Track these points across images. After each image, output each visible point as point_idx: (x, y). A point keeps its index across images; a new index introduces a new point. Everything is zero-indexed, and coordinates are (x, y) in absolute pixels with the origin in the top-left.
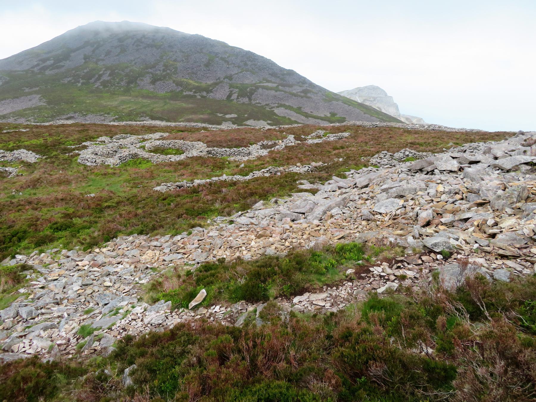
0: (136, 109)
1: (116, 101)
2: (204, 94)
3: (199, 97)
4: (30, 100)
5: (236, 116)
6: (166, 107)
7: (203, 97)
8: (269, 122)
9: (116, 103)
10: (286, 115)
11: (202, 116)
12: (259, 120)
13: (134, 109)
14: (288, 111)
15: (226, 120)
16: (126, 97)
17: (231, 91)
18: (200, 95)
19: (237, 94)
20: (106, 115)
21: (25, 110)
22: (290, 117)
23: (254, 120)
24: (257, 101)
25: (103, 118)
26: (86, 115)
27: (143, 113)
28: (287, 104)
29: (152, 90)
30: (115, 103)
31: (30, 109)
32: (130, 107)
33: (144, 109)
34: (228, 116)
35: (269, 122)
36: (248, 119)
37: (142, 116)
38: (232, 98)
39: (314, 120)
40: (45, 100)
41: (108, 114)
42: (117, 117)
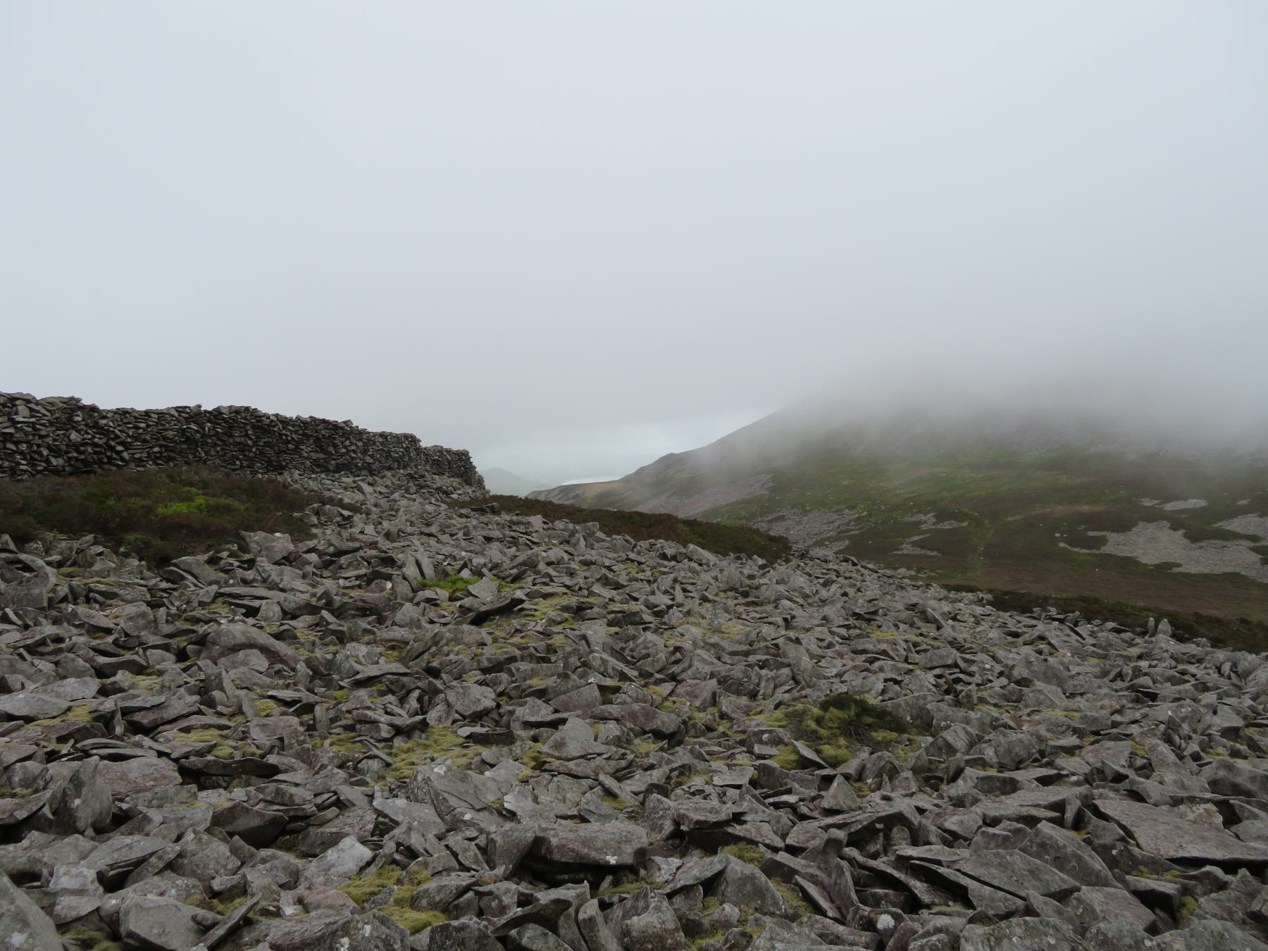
11: (1086, 508)
15: (1152, 517)
23: (1261, 516)
26: (805, 513)
34: (1169, 507)
36: (1243, 511)
41: (852, 508)
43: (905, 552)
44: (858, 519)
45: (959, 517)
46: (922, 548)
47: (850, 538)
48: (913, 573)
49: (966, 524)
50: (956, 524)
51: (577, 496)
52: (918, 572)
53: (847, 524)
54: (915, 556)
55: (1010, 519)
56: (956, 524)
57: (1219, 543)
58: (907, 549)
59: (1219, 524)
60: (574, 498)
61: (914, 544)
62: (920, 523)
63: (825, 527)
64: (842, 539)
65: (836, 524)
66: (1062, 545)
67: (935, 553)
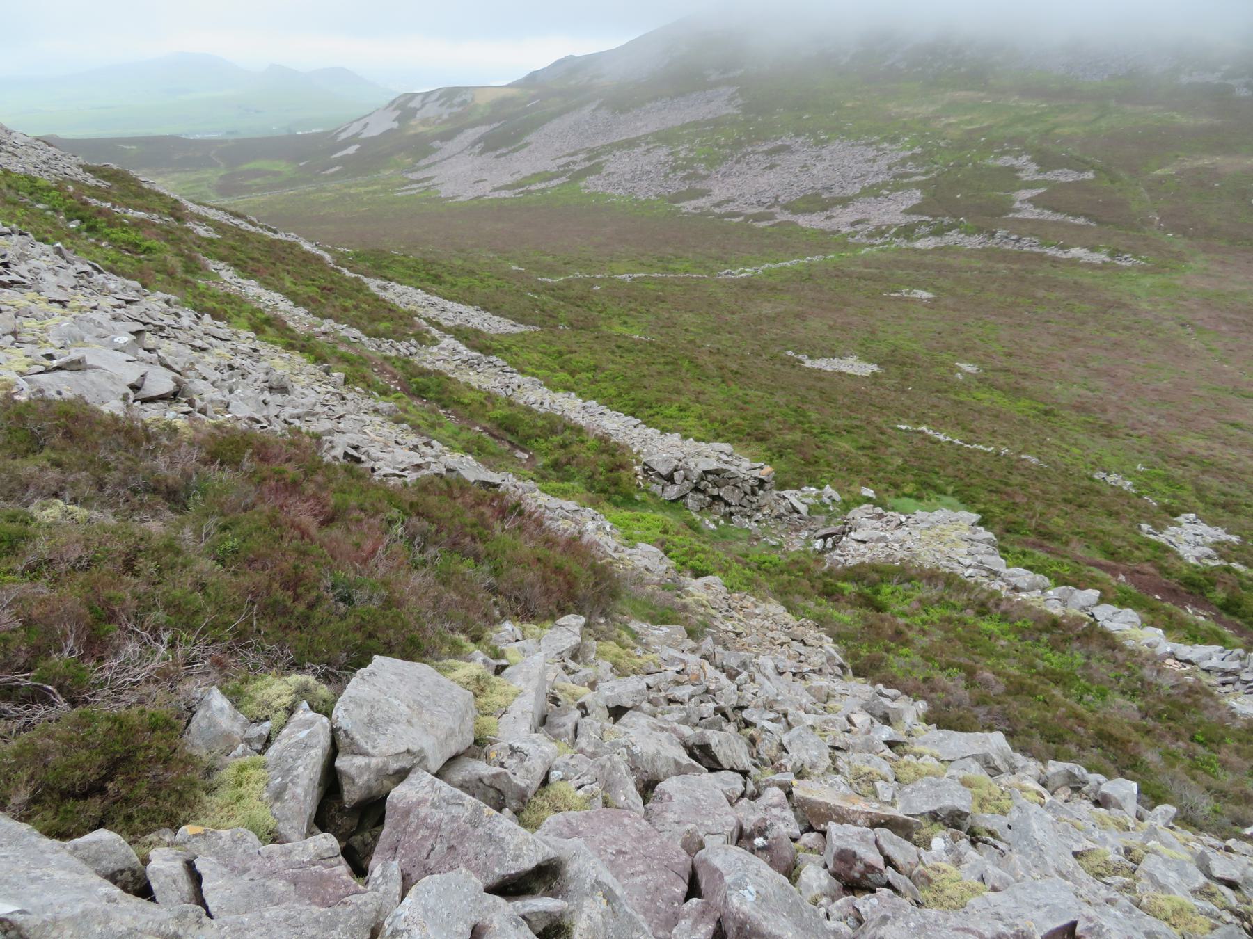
0: (990, 127)
4: (709, 101)
6: (1103, 124)
9: (931, 109)
13: (981, 129)
16: (971, 94)
20: (886, 145)
21: (683, 127)
25: (871, 153)
26: (822, 143)
27: (1012, 140)
30: (926, 110)
31: (696, 124)
32: (970, 122)
33: (1020, 128)
37: (1004, 153)
40: (740, 101)
41: (894, 140)
42: (918, 150)
43: (1028, 215)
44: (913, 158)
45: (1078, 164)
46: (1056, 210)
47: (918, 185)
48: (1100, 257)
49: (1090, 175)
50: (1073, 176)
51: (464, 102)
52: (1114, 254)
53: (903, 162)
54: (1056, 223)
55: (1160, 172)
56: (1073, 176)
58: (1030, 213)
60: (460, 104)
61: (1035, 202)
62: (1013, 170)
63: (865, 167)
64: (908, 187)
65: (883, 163)
67: (1081, 221)
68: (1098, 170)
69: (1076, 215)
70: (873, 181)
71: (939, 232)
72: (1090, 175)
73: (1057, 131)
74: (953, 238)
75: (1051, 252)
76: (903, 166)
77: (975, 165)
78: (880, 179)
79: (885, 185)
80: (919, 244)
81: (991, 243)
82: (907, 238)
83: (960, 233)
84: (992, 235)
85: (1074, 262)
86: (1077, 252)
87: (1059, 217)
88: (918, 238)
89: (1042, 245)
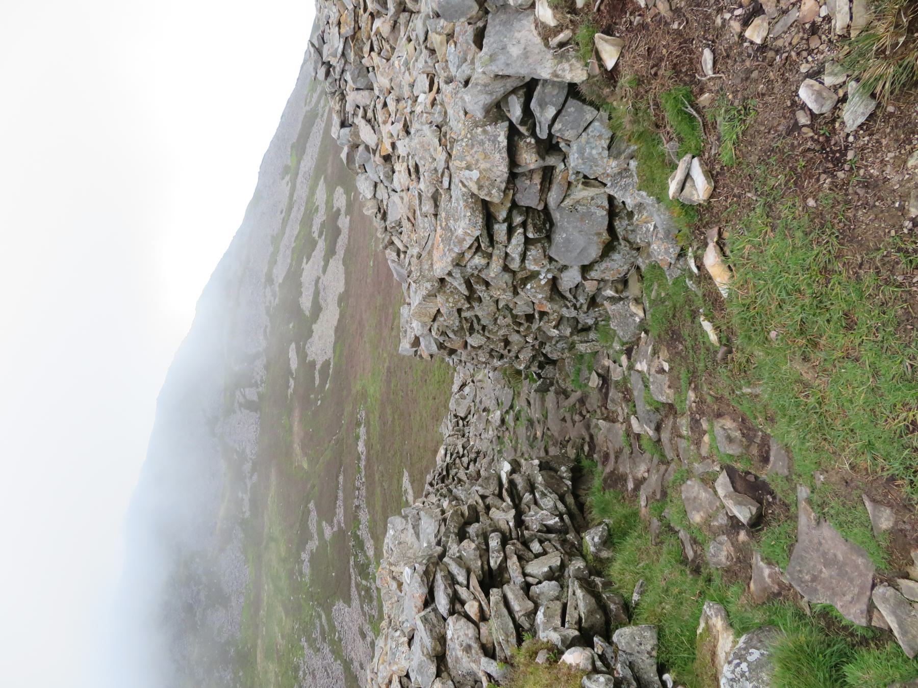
1: (266, 672)
2: (248, 466)
3: (255, 477)
5: (293, 346)
7: (254, 470)
8: (305, 261)
9: (271, 666)
10: (289, 252)
12: (301, 283)
14: (280, 259)
16: (258, 651)
17: (241, 405)
18: (251, 477)
19: (247, 390)
22: (293, 239)
24: (261, 338)
25: (309, 678)
28: (265, 270)
29: (242, 600)
35: (305, 261)
37: (301, 573)
38: (255, 398)
39: (298, 186)
46: (336, 498)
48: (362, 430)
52: (358, 424)
57: (322, 293)
59: (307, 313)
66: (327, 386)
67: (341, 478)
68: (308, 502)
69: (338, 483)
70: (330, 655)
71: (360, 544)
72: (311, 505)
73: (283, 554)
74: (363, 533)
75: (363, 463)
76: (315, 640)
77: (310, 587)
78: (327, 650)
79: (332, 642)
80: (371, 553)
81: (364, 505)
82: (368, 566)
83: (359, 529)
84: (358, 507)
85: (368, 445)
86: (361, 447)
87: (341, 494)
88: (367, 557)
89: (360, 472)
